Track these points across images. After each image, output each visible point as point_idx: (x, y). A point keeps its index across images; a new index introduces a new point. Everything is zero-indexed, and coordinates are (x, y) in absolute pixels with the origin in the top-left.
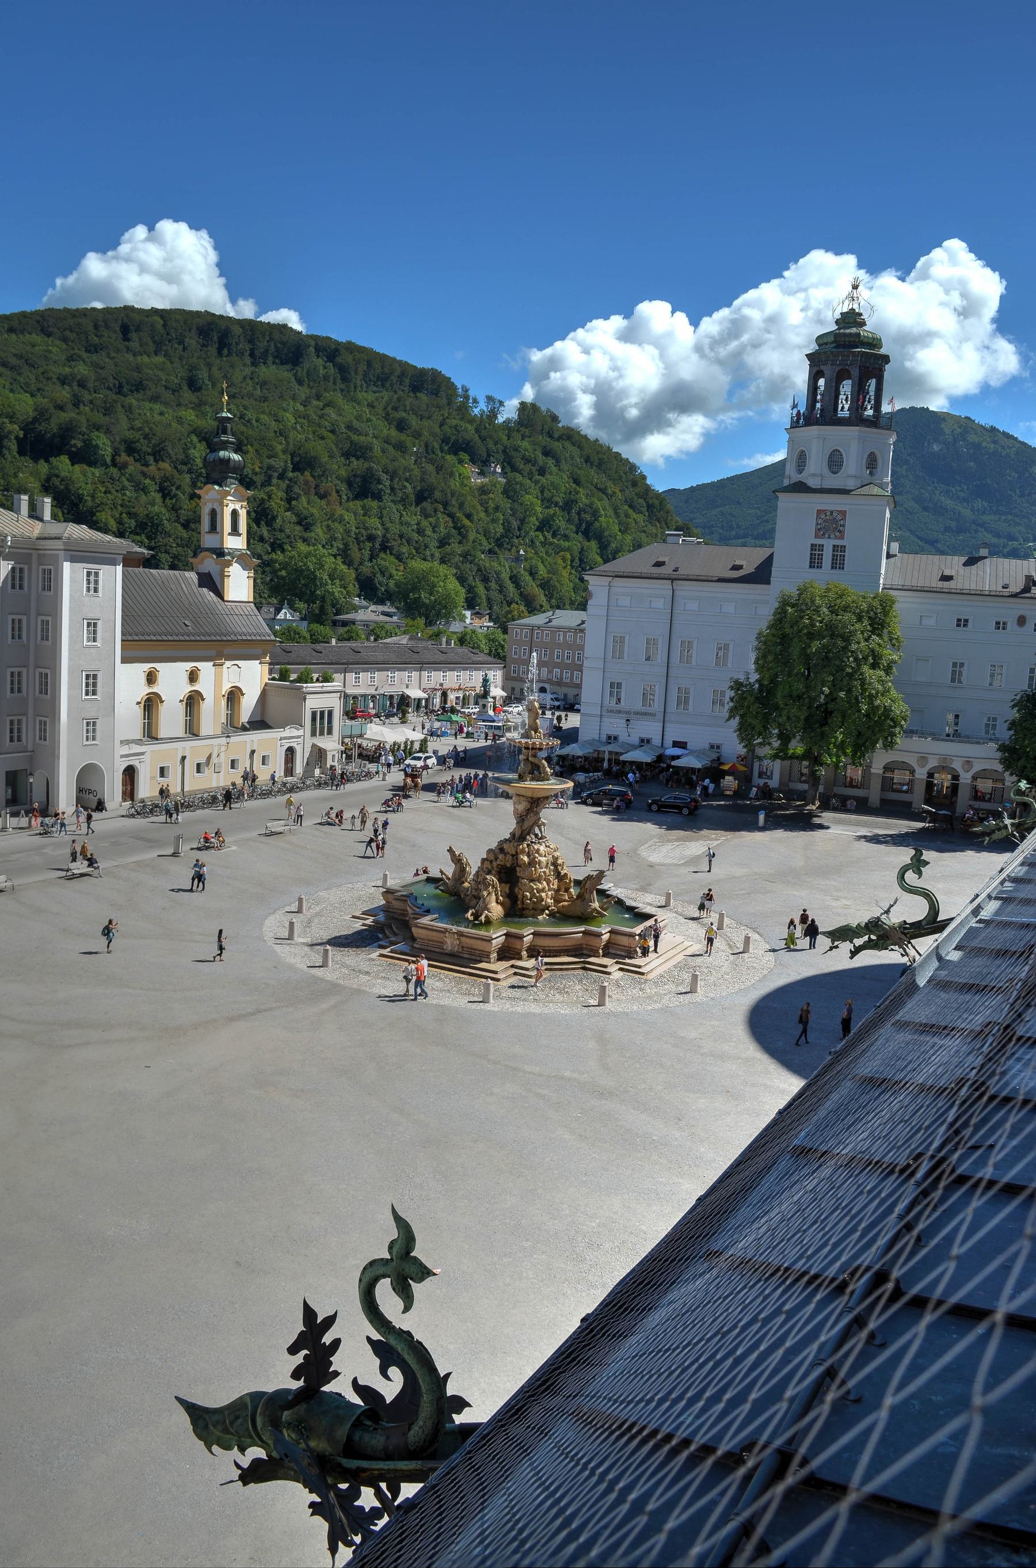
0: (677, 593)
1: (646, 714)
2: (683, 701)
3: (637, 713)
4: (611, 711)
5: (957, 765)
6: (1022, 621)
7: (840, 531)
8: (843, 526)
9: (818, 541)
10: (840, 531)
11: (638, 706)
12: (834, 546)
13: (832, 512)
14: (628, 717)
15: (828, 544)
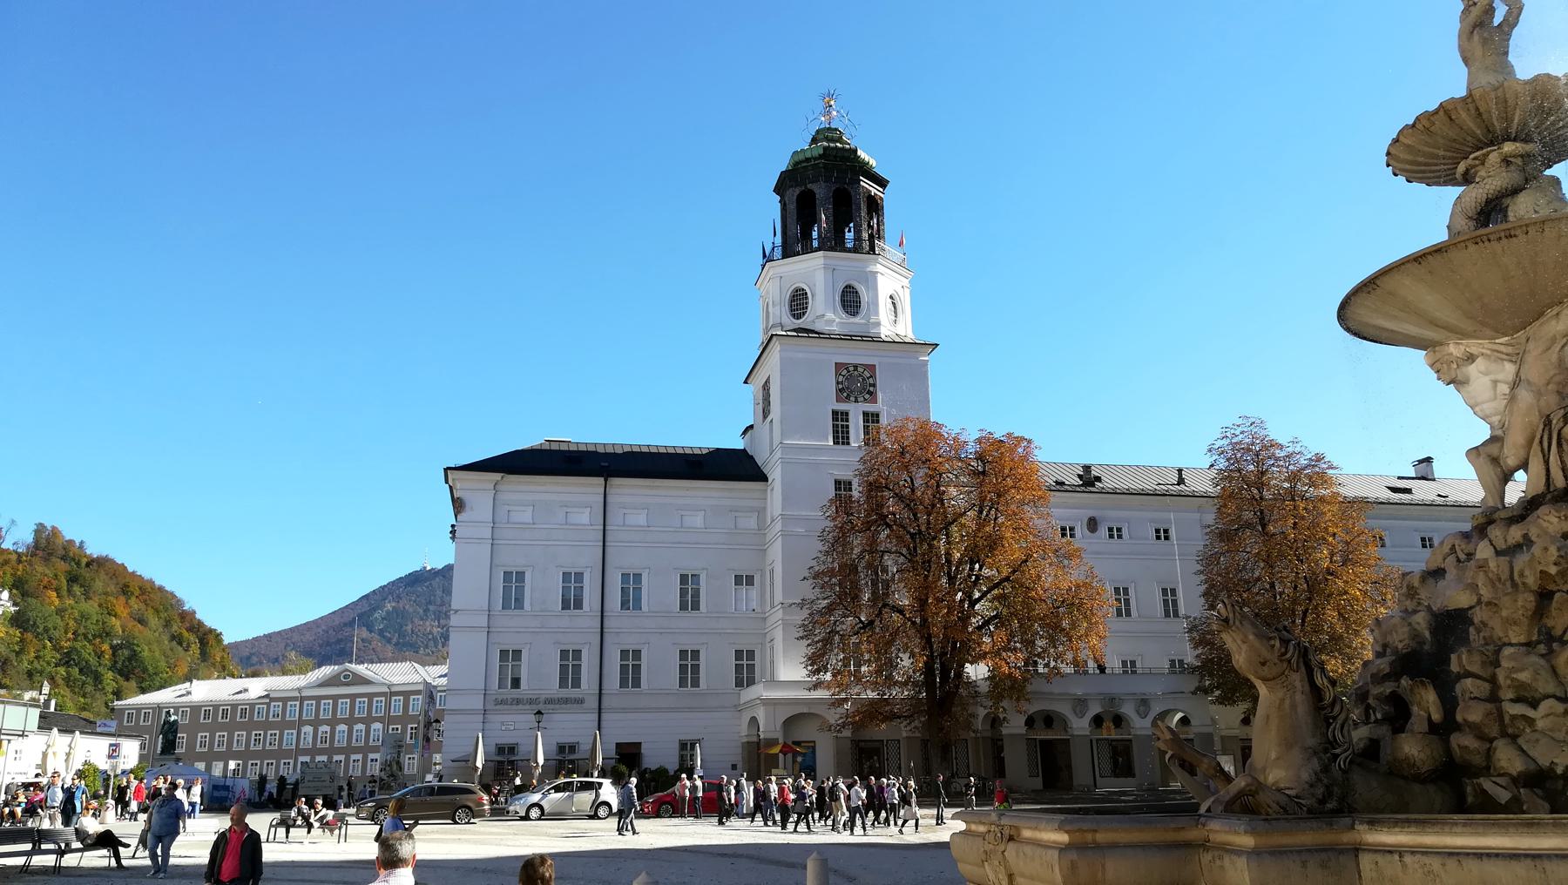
0: (609, 499)
1: (566, 701)
2: (631, 675)
3: (549, 701)
4: (503, 702)
5: (1128, 710)
6: (1093, 524)
7: (870, 393)
8: (874, 385)
9: (842, 407)
10: (870, 393)
11: (552, 686)
12: (865, 414)
13: (856, 367)
14: (536, 708)
15: (856, 412)
